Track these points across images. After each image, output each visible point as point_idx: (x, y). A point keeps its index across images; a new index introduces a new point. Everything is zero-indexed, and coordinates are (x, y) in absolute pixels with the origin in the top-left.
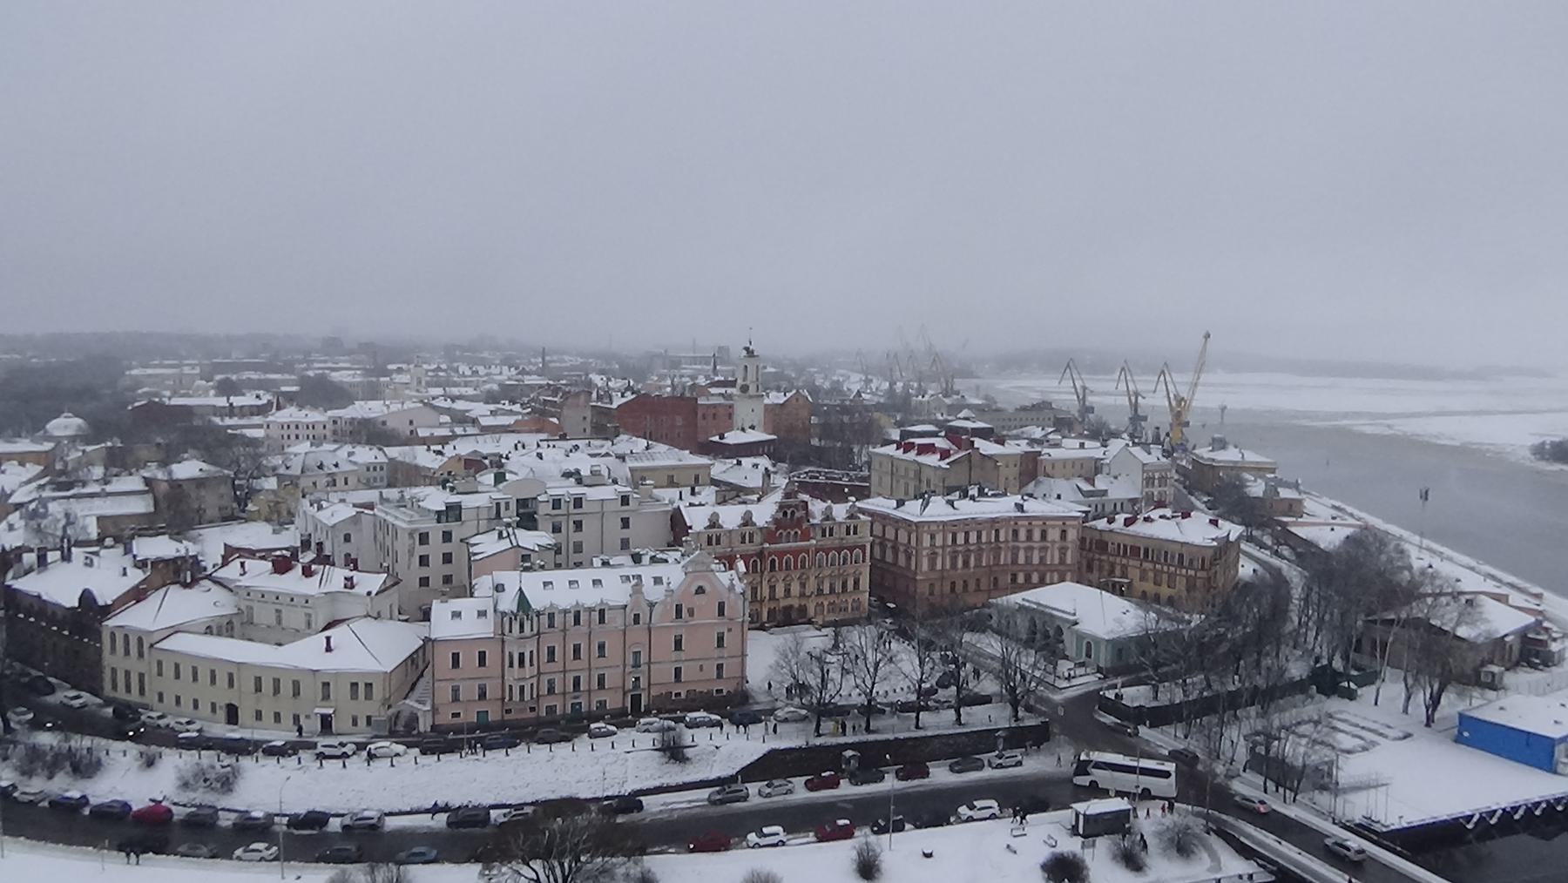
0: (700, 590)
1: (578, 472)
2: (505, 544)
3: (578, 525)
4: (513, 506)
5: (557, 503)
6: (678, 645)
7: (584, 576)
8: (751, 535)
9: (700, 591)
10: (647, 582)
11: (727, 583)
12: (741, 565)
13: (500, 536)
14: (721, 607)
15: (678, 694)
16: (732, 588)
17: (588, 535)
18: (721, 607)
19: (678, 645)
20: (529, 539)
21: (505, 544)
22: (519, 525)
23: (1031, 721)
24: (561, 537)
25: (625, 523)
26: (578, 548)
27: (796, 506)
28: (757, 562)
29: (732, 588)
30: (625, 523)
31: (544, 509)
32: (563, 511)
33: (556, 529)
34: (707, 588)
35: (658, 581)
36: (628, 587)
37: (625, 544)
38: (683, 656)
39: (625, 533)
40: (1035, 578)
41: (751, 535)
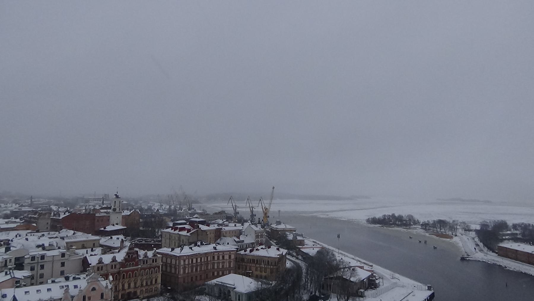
0: (94, 289)
1: (43, 245)
2: (8, 277)
3: (42, 267)
4: (13, 260)
5: (33, 258)
7: (43, 288)
8: (115, 266)
10: (71, 287)
11: (105, 285)
12: (111, 278)
13: (6, 274)
14: (102, 295)
16: (107, 287)
17: (46, 271)
18: (102, 295)
20: (19, 274)
21: (8, 277)
22: (16, 269)
24: (34, 272)
25: (63, 264)
26: (42, 276)
27: (133, 253)
28: (117, 276)
29: (107, 287)
30: (63, 264)
31: (27, 261)
32: (36, 261)
33: (32, 269)
34: (97, 288)
35: (76, 287)
36: (63, 290)
37: (62, 273)
39: (62, 269)
40: (221, 273)
41: (115, 266)
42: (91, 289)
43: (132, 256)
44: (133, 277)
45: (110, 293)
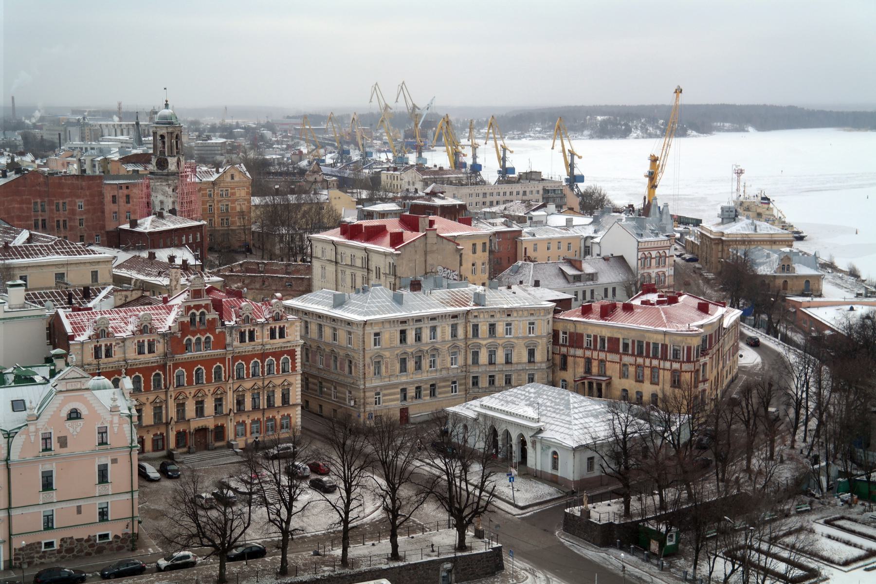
0: (74, 415)
6: (47, 485)
9: (74, 415)
11: (108, 404)
12: (127, 383)
14: (103, 432)
15: (50, 544)
16: (114, 410)
18: (103, 432)
19: (47, 485)
23: (481, 548)
27: (206, 307)
28: (147, 379)
29: (114, 410)
34: (84, 411)
38: (53, 496)
40: (484, 383)
41: (151, 345)
42: (64, 413)
43: (203, 314)
44: (190, 383)
45: (127, 427)
